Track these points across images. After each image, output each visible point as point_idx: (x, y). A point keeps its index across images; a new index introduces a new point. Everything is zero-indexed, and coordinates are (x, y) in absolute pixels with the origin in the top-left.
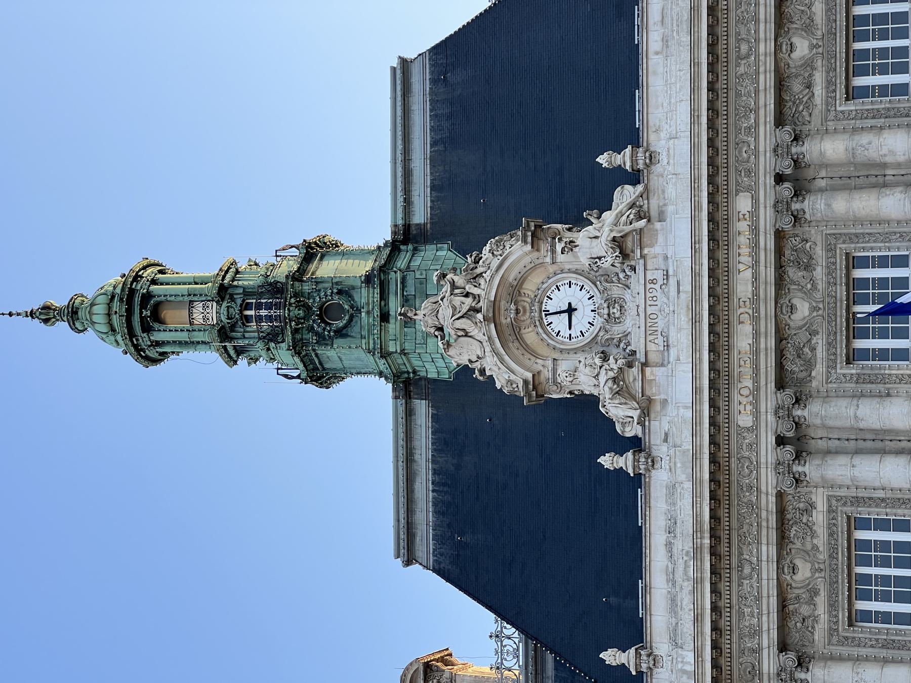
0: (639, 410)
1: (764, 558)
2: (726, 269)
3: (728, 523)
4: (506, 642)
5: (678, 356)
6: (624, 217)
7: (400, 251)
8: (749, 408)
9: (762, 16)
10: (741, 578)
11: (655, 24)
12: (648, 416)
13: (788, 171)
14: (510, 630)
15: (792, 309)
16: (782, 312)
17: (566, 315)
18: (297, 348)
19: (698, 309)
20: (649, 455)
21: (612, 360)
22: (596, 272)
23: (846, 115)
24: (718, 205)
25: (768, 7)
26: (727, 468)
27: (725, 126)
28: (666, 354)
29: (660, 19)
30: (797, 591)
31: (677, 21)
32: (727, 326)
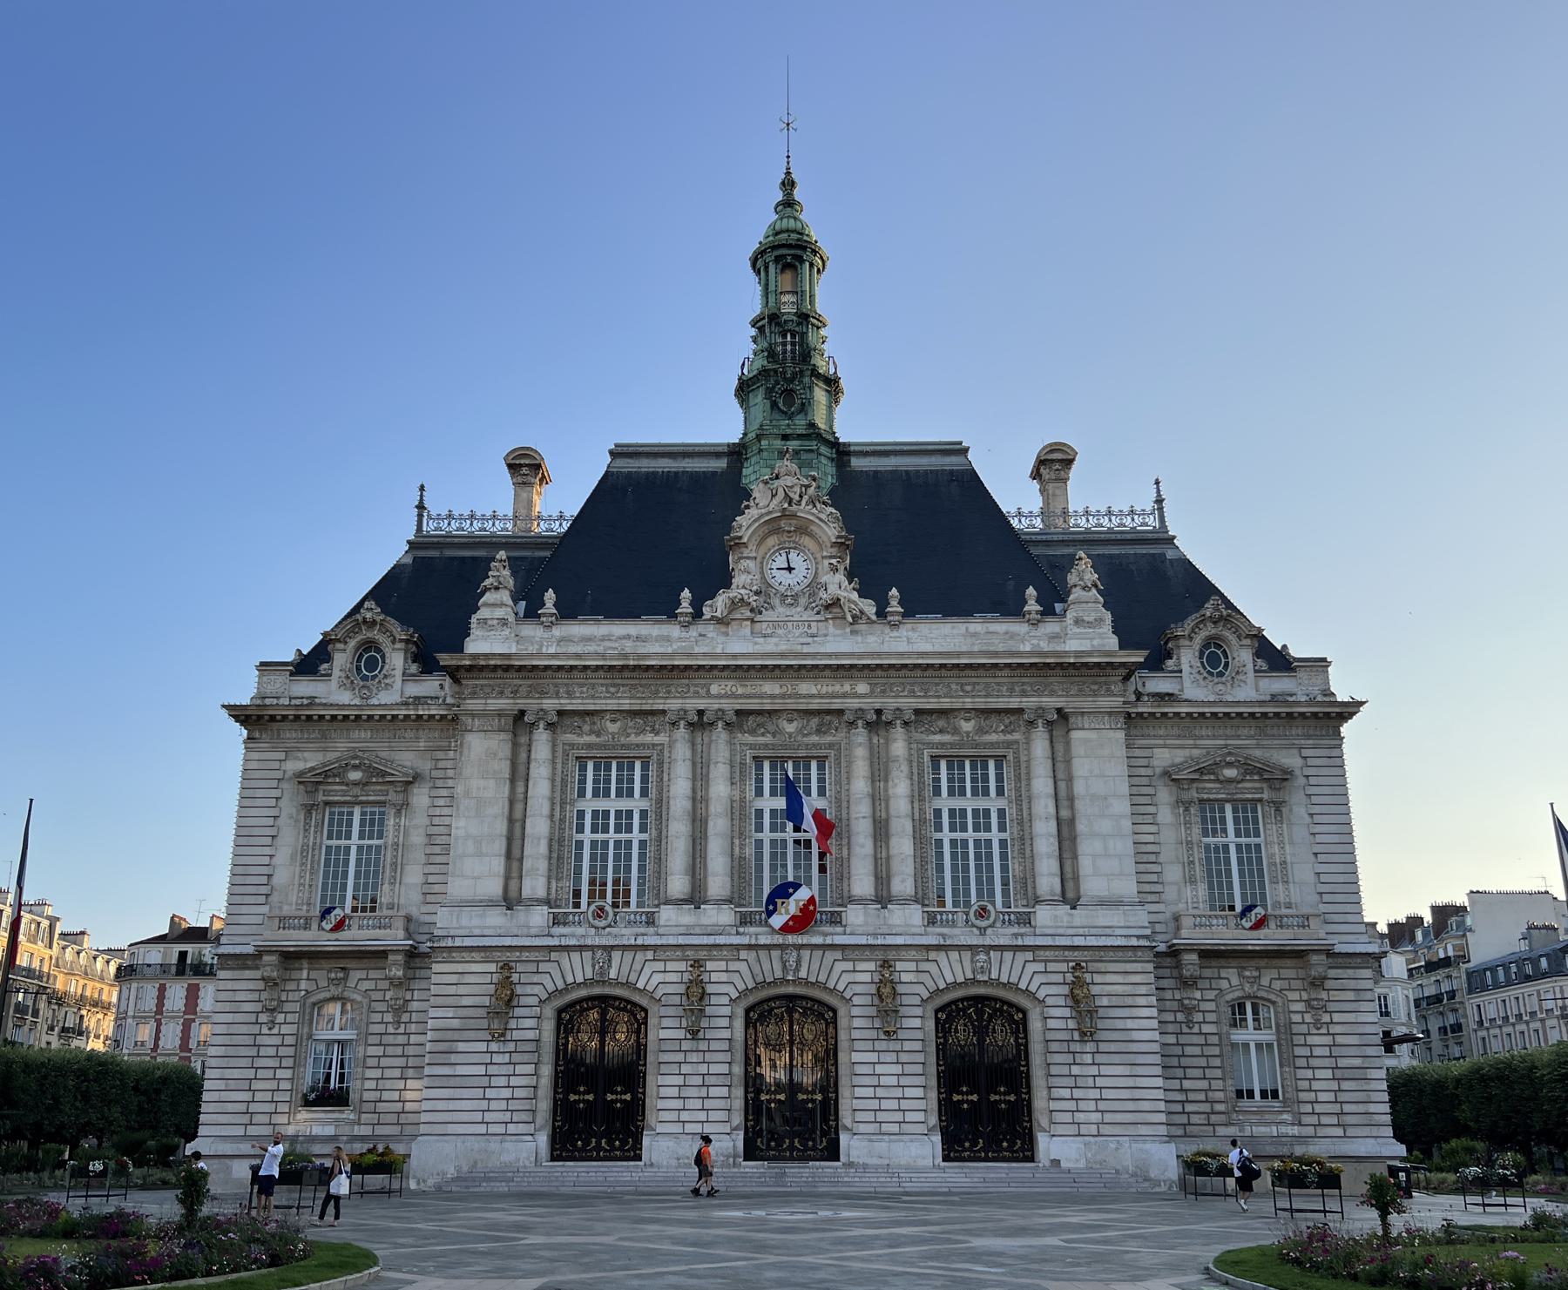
1: (621, 701)
4: (558, 523)
7: (832, 448)
8: (723, 692)
10: (607, 685)
13: (883, 718)
14: (566, 526)
15: (790, 721)
18: (764, 373)
21: (755, 598)
23: (921, 756)
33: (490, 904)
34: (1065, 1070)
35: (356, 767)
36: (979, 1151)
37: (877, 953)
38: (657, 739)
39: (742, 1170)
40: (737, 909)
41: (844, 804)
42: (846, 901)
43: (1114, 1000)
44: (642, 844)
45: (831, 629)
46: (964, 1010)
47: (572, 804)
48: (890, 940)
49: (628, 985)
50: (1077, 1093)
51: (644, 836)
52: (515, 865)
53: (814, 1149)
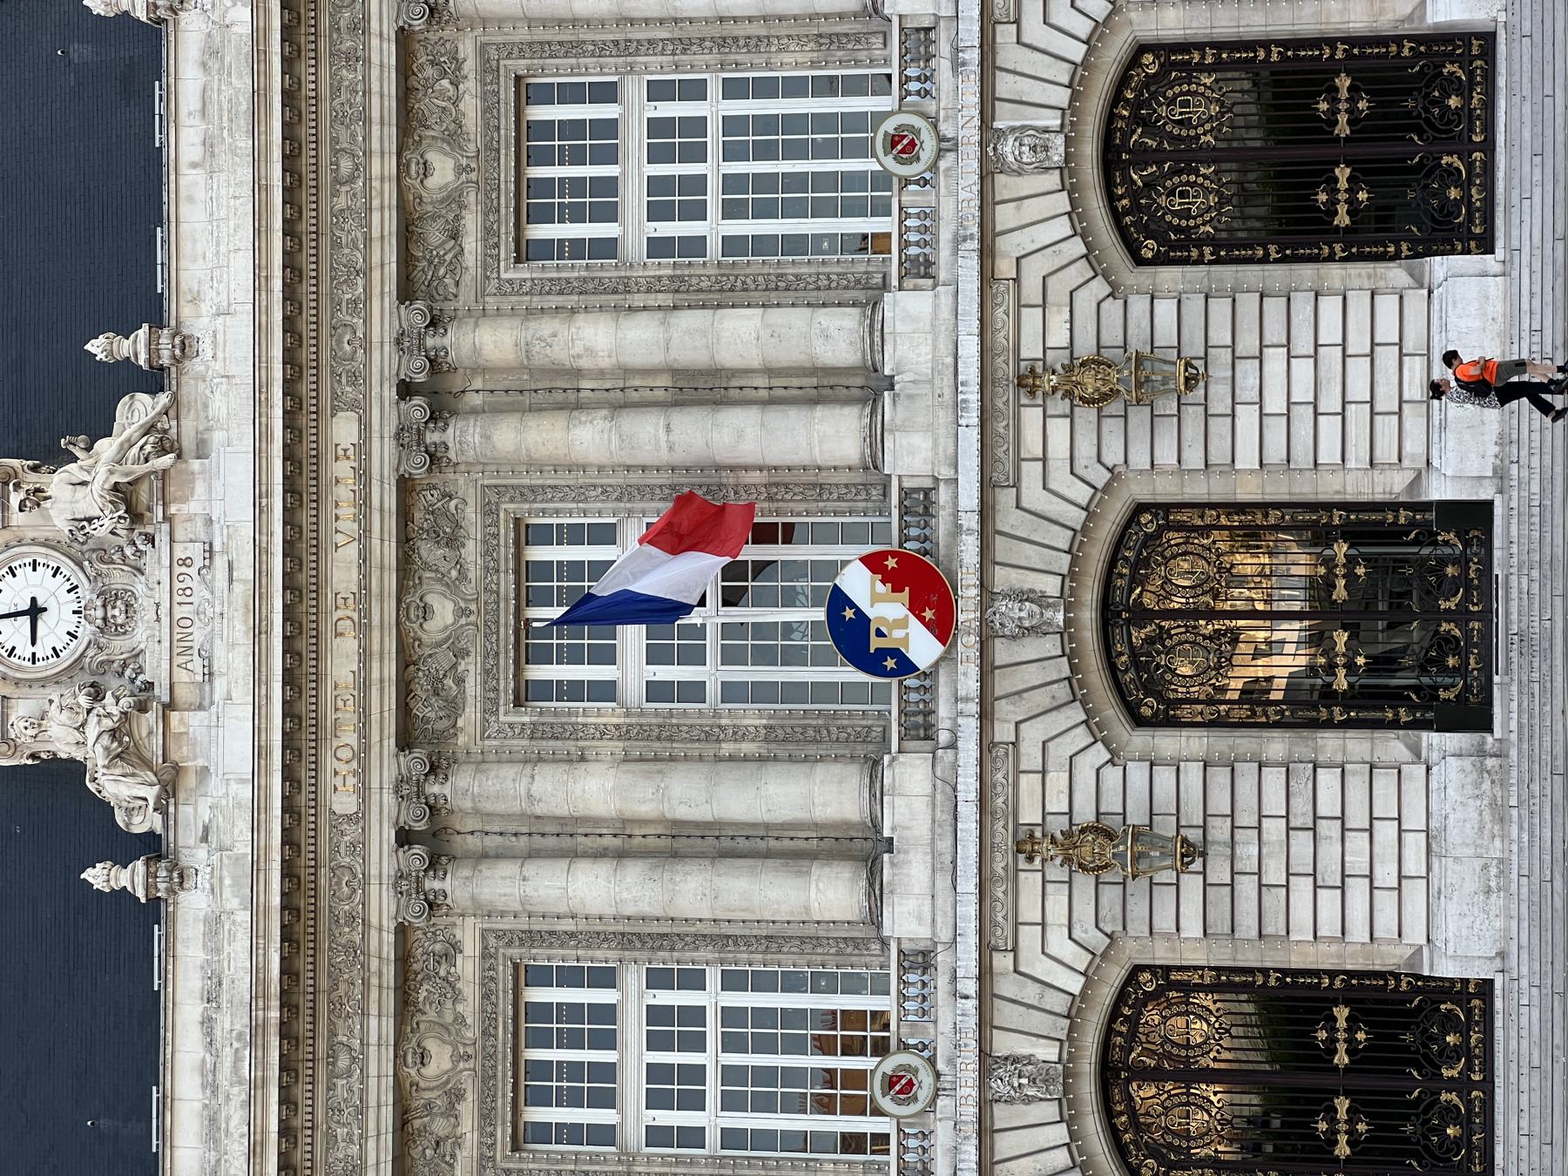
0: (157, 787)
1: (373, 1039)
2: (314, 542)
3: (311, 982)
5: (229, 692)
6: (135, 450)
8: (351, 781)
9: (375, 114)
10: (332, 1075)
11: (190, 114)
12: (174, 796)
13: (421, 378)
15: (426, 612)
16: (408, 618)
17: (26, 620)
19: (264, 611)
20: (174, 865)
21: (109, 699)
22: (83, 544)
23: (516, 287)
24: (301, 432)
25: (386, 98)
26: (313, 886)
27: (314, 297)
28: (207, 688)
29: (198, 106)
30: (427, 1095)
31: (230, 111)
32: (314, 641)
36: (1470, 166)
37: (1000, 404)
38: (470, 944)
39: (1514, 737)
40: (894, 747)
41: (635, 478)
42: (873, 477)
44: (732, 982)
45: (193, 507)
46: (1134, 195)
47: (627, 1157)
48: (970, 371)
49: (1073, 1016)
51: (713, 977)
53: (1462, 561)
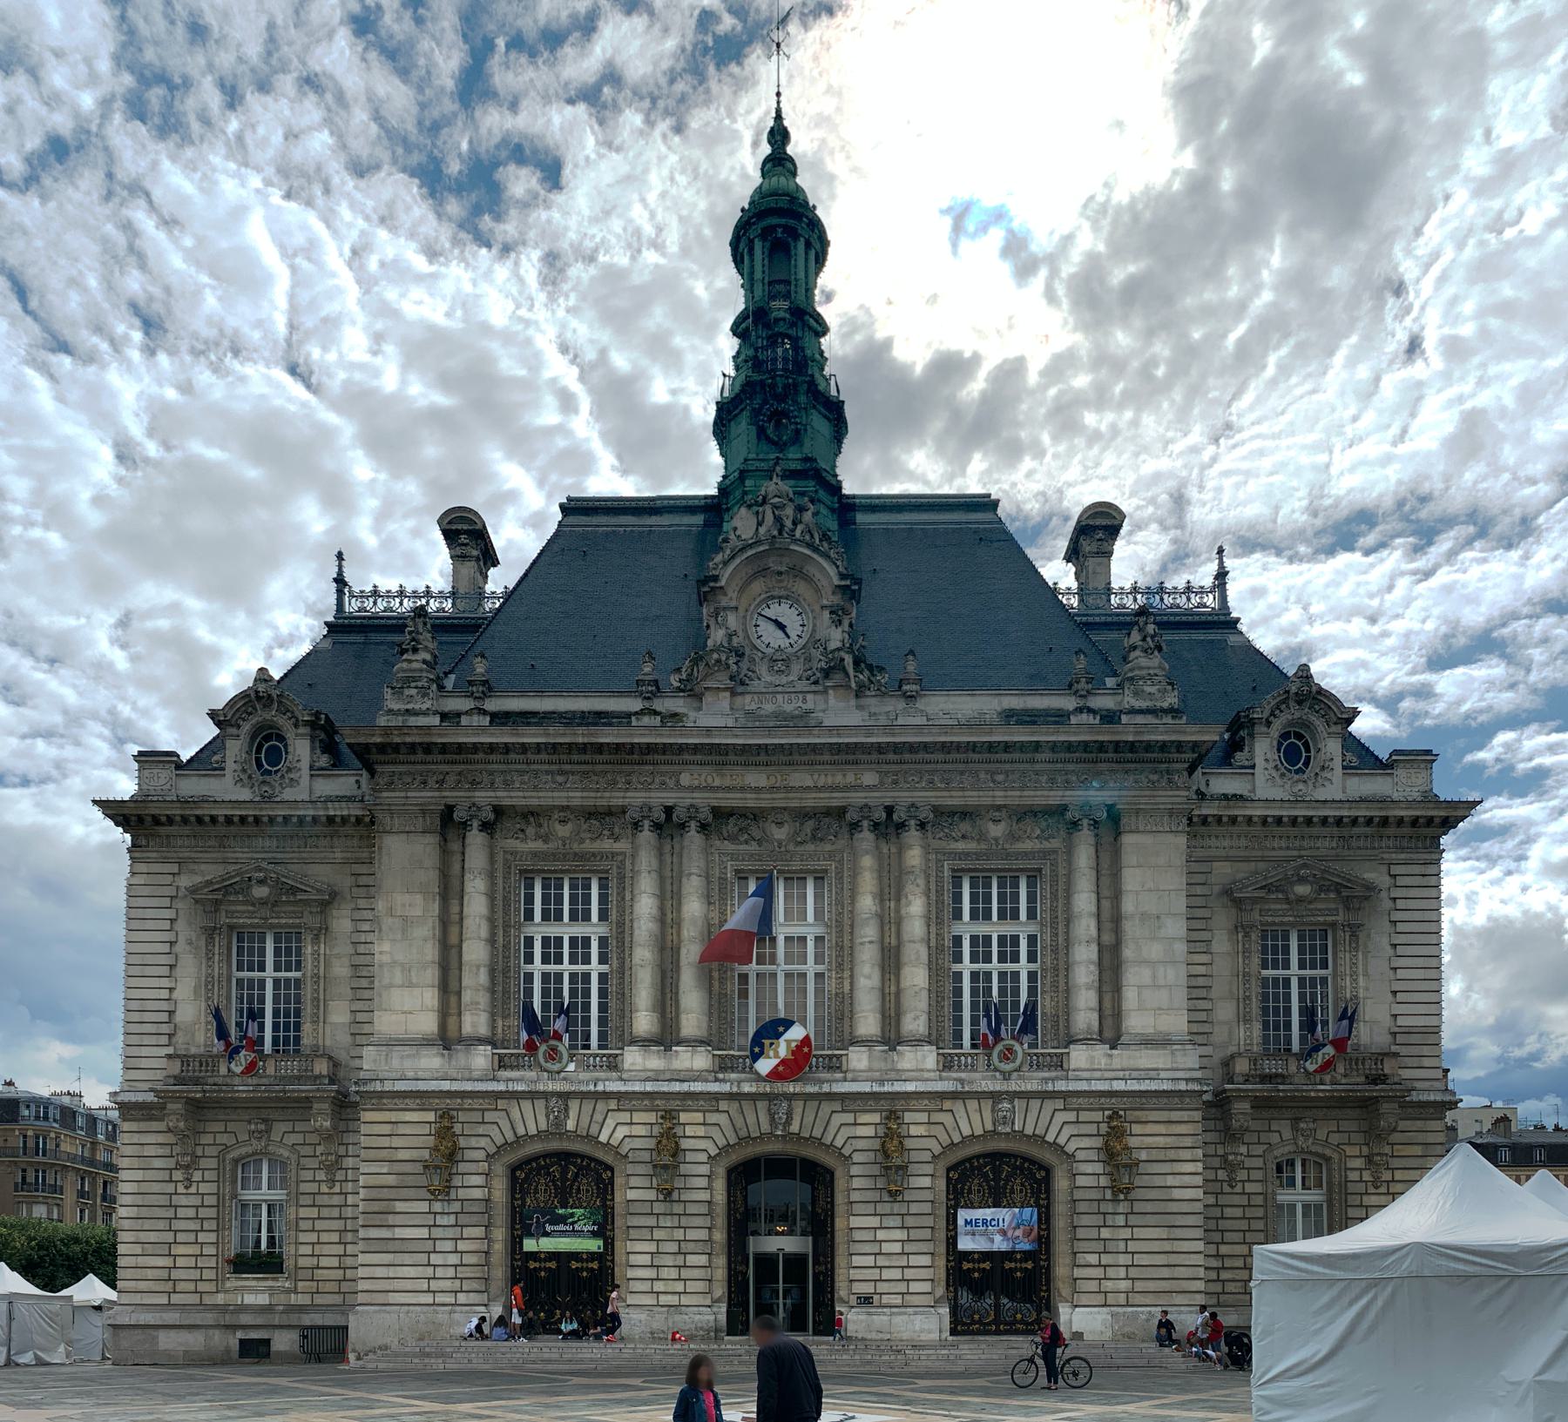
23: (940, 869)
33: (426, 1042)
34: (1093, 1233)
35: (261, 882)
36: (989, 1324)
41: (847, 929)
43: (1155, 1155)
44: (603, 978)
46: (980, 1168)
47: (519, 926)
48: (898, 1087)
50: (1105, 1259)
52: (453, 999)
